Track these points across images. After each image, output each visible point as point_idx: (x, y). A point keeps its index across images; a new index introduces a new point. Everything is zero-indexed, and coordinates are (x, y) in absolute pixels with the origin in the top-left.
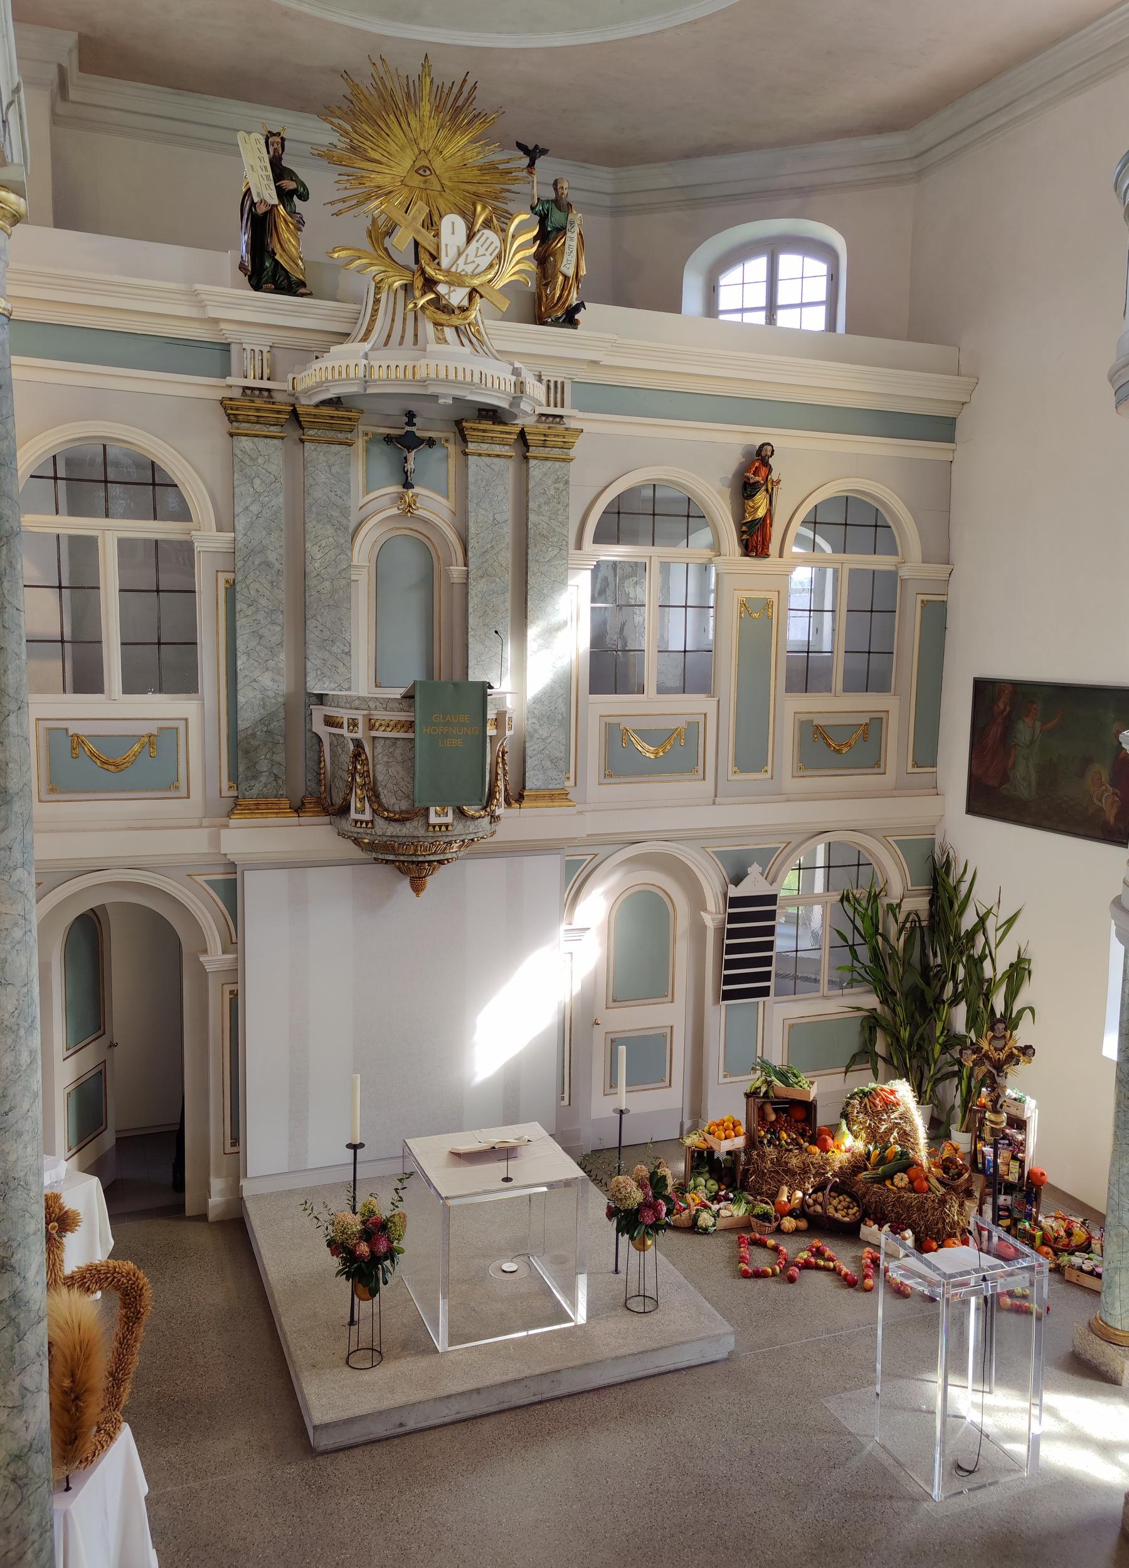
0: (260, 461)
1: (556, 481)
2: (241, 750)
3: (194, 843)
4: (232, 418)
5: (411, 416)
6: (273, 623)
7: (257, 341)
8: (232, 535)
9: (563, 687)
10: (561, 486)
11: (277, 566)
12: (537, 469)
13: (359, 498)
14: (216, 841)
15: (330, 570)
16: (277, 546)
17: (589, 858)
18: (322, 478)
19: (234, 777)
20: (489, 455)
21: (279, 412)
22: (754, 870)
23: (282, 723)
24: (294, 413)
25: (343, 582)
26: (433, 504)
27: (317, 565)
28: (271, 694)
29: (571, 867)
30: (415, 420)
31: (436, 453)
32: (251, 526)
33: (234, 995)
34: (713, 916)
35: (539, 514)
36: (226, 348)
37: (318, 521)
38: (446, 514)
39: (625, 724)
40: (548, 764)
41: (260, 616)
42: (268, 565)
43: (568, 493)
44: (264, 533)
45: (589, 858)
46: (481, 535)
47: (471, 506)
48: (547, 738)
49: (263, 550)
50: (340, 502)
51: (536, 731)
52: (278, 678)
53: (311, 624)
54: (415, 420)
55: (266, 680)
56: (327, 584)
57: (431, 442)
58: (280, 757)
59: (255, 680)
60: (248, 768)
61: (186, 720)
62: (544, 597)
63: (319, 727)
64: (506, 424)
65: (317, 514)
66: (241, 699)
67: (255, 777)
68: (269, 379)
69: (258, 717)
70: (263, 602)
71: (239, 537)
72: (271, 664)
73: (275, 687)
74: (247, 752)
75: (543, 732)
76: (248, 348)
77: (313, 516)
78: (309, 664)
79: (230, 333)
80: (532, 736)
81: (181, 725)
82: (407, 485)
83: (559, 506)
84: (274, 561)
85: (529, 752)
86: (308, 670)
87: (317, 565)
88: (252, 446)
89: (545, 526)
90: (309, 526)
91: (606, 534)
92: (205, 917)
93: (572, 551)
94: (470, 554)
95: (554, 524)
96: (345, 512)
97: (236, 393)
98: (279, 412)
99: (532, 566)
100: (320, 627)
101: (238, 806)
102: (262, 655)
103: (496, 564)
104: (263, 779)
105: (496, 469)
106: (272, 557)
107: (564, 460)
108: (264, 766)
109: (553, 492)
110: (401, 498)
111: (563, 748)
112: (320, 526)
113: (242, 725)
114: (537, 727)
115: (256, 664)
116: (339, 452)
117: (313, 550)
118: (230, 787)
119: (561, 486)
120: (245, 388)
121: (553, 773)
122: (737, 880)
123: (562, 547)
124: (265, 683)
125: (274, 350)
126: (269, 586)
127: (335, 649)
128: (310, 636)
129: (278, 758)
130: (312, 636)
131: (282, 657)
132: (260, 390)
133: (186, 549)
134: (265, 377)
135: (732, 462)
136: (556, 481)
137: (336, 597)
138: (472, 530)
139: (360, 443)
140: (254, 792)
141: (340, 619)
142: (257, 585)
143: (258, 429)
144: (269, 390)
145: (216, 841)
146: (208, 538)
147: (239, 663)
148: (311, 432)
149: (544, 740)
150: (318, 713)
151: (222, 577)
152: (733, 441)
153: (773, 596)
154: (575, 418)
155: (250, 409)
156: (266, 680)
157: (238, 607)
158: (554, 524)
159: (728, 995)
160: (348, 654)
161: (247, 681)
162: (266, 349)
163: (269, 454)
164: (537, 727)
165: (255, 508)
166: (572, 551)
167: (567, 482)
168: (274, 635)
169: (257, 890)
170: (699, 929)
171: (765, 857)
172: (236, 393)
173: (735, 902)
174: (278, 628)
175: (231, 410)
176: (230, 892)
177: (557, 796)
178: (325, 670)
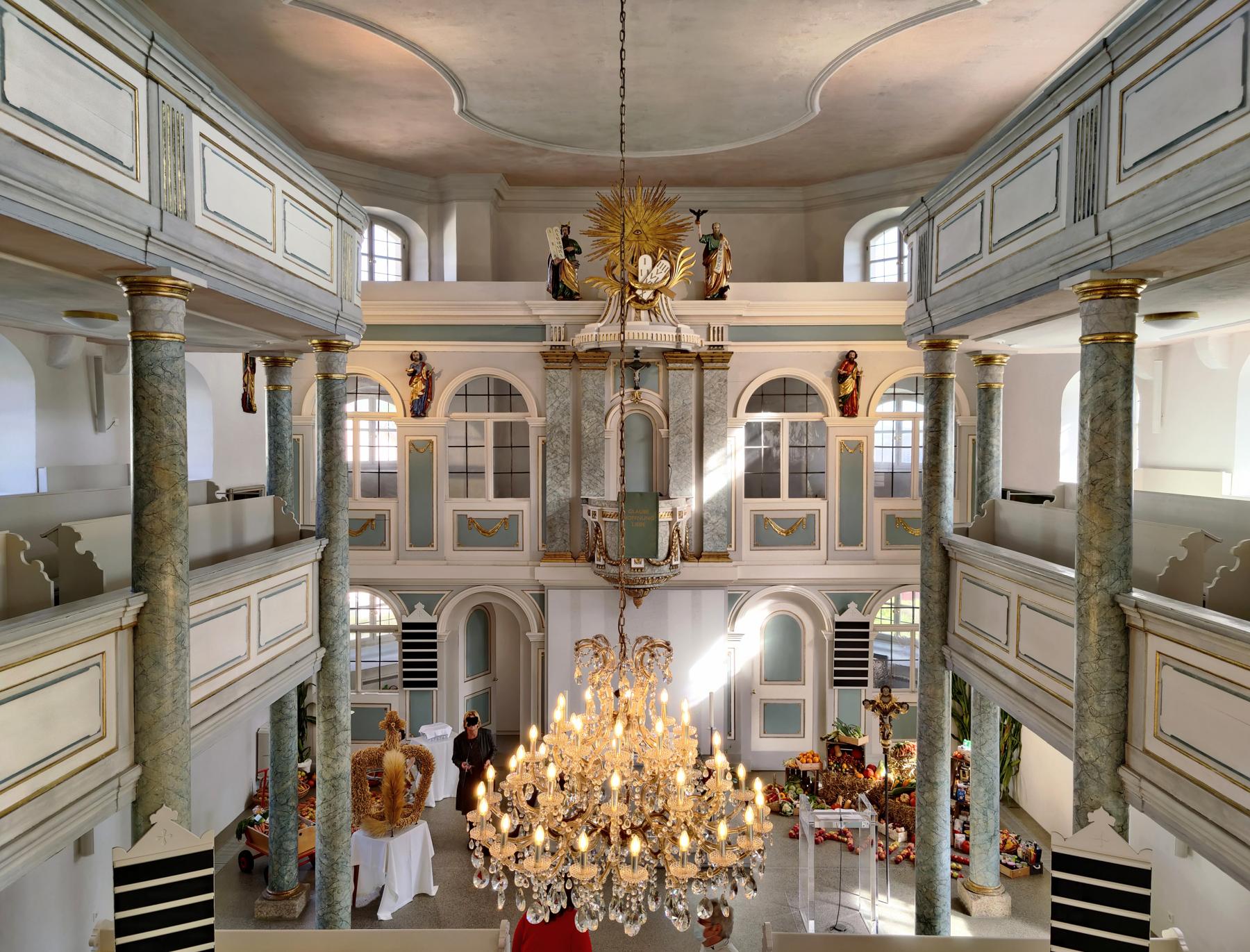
2: (548, 525)
3: (522, 574)
4: (546, 361)
7: (558, 323)
9: (728, 493)
12: (708, 375)
14: (533, 573)
18: (590, 387)
19: (544, 541)
22: (852, 606)
26: (651, 398)
29: (732, 599)
31: (652, 370)
34: (828, 632)
35: (709, 398)
38: (658, 402)
39: (766, 515)
42: (562, 432)
49: (560, 425)
53: (584, 462)
55: (560, 491)
57: (648, 365)
58: (567, 531)
62: (712, 444)
63: (585, 515)
75: (714, 519)
79: (544, 321)
82: (637, 388)
85: (705, 530)
91: (753, 407)
96: (602, 403)
99: (706, 428)
101: (549, 556)
106: (564, 428)
108: (559, 535)
110: (633, 394)
113: (548, 514)
117: (585, 424)
121: (719, 543)
122: (841, 612)
123: (724, 416)
124: (561, 492)
131: (570, 480)
135: (833, 362)
138: (671, 409)
139: (611, 368)
145: (533, 573)
146: (535, 421)
150: (586, 508)
151: (541, 439)
152: (834, 349)
153: (864, 440)
154: (730, 346)
156: (560, 491)
159: (837, 683)
163: (564, 377)
165: (556, 405)
166: (730, 417)
169: (553, 597)
170: (819, 640)
171: (862, 600)
172: (547, 349)
173: (838, 625)
175: (545, 356)
176: (541, 600)
177: (723, 556)
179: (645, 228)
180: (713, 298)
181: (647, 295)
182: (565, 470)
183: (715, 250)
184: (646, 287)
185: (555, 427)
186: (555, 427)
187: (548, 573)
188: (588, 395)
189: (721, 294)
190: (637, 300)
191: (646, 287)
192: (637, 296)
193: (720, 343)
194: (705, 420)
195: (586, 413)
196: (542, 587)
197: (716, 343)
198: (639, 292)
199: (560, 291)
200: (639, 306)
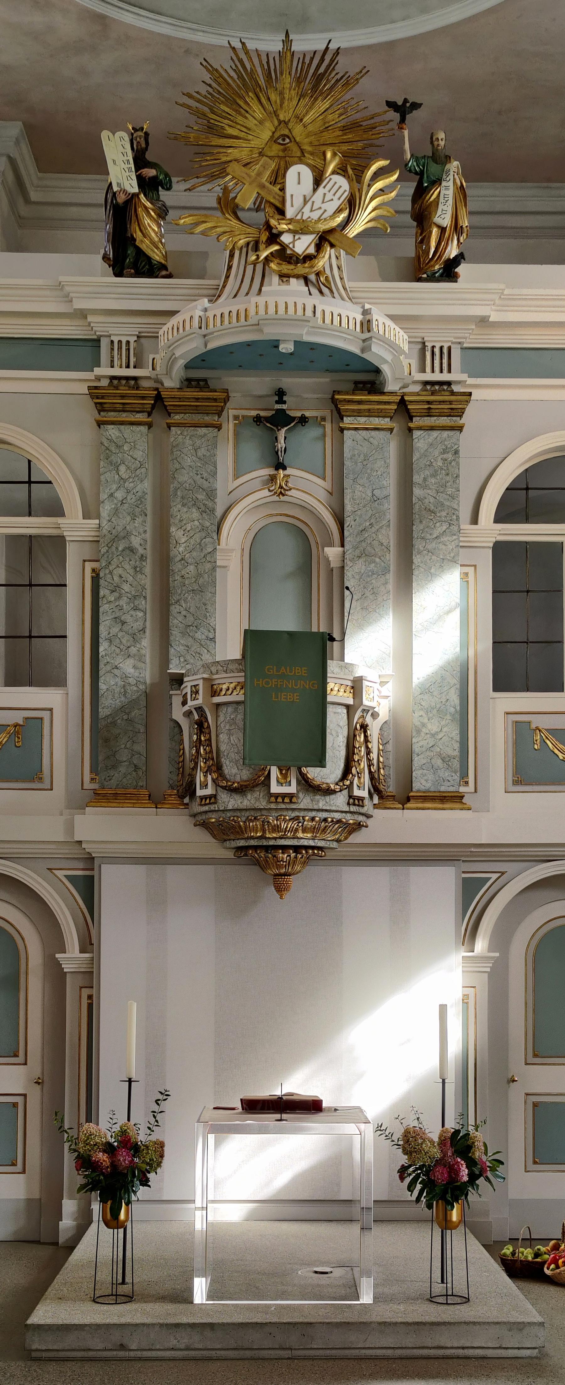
0: (126, 448)
1: (444, 452)
4: (101, 408)
5: (280, 394)
6: (136, 609)
8: (97, 521)
10: (449, 456)
11: (141, 551)
12: (421, 440)
13: (225, 481)
14: (70, 827)
15: (194, 554)
16: (141, 530)
17: (495, 876)
18: (188, 461)
20: (367, 429)
21: (143, 398)
23: (143, 711)
24: (159, 398)
25: (208, 566)
27: (181, 549)
28: (132, 681)
30: (285, 398)
32: (116, 512)
33: (90, 1006)
35: (424, 486)
36: (95, 343)
37: (183, 505)
38: (323, 495)
39: (537, 721)
40: (439, 762)
41: (123, 602)
42: (132, 550)
43: (458, 464)
44: (129, 518)
45: (495, 876)
46: (359, 513)
47: (347, 483)
48: (437, 733)
49: (127, 535)
50: (206, 485)
51: (424, 725)
52: (140, 665)
53: (174, 609)
54: (285, 398)
55: (128, 667)
56: (191, 568)
58: (140, 747)
59: (116, 667)
60: (108, 757)
61: (51, 710)
63: (178, 713)
64: (383, 393)
65: (183, 498)
66: (102, 687)
67: (114, 767)
68: (135, 367)
69: (118, 703)
70: (126, 587)
71: (104, 523)
72: (133, 650)
73: (137, 674)
74: (106, 740)
75: (433, 727)
76: (116, 339)
77: (179, 499)
78: (172, 651)
80: (419, 731)
81: (45, 715)
83: (448, 478)
84: (137, 546)
86: (171, 657)
87: (181, 549)
88: (117, 434)
89: (432, 500)
90: (174, 510)
92: (63, 913)
93: (466, 526)
94: (346, 533)
95: (441, 497)
96: (211, 494)
97: (105, 383)
98: (143, 398)
100: (184, 613)
102: (124, 641)
103: (375, 543)
104: (123, 769)
105: (375, 443)
106: (136, 541)
107: (452, 428)
108: (124, 756)
109: (440, 463)
110: (273, 479)
111: (457, 746)
112: (185, 510)
113: (103, 712)
114: (426, 721)
115: (118, 651)
116: (205, 435)
118: (92, 779)
119: (449, 456)
120: (113, 378)
125: (142, 340)
126: (132, 571)
127: (198, 635)
128: (174, 622)
129: (137, 747)
130: (175, 621)
131: (146, 644)
132: (127, 378)
133: (58, 542)
134: (132, 364)
136: (444, 452)
137: (201, 581)
138: (348, 507)
140: (113, 782)
141: (205, 604)
142: (120, 571)
143: (124, 417)
144: (135, 379)
145: (70, 827)
146: (75, 526)
147: (101, 649)
148: (177, 417)
149: (433, 735)
151: (89, 566)
155: (115, 396)
156: (128, 667)
157: (102, 593)
158: (441, 497)
160: (213, 640)
161: (108, 668)
162: (132, 339)
164: (426, 721)
165: (119, 495)
167: (456, 452)
168: (137, 621)
169: (111, 880)
172: (105, 383)
174: (140, 614)
176: (87, 888)
178: (188, 657)
179: (298, 131)
180: (432, 278)
181: (303, 245)
182: (138, 625)
183: (437, 182)
184: (301, 229)
185: (117, 539)
186: (117, 539)
187: (102, 827)
188: (184, 477)
189: (449, 272)
190: (285, 255)
191: (301, 229)
192: (284, 247)
193: (445, 377)
194: (417, 528)
195: (178, 510)
196: (90, 859)
197: (437, 377)
198: (286, 239)
199: (127, 258)
200: (286, 268)
